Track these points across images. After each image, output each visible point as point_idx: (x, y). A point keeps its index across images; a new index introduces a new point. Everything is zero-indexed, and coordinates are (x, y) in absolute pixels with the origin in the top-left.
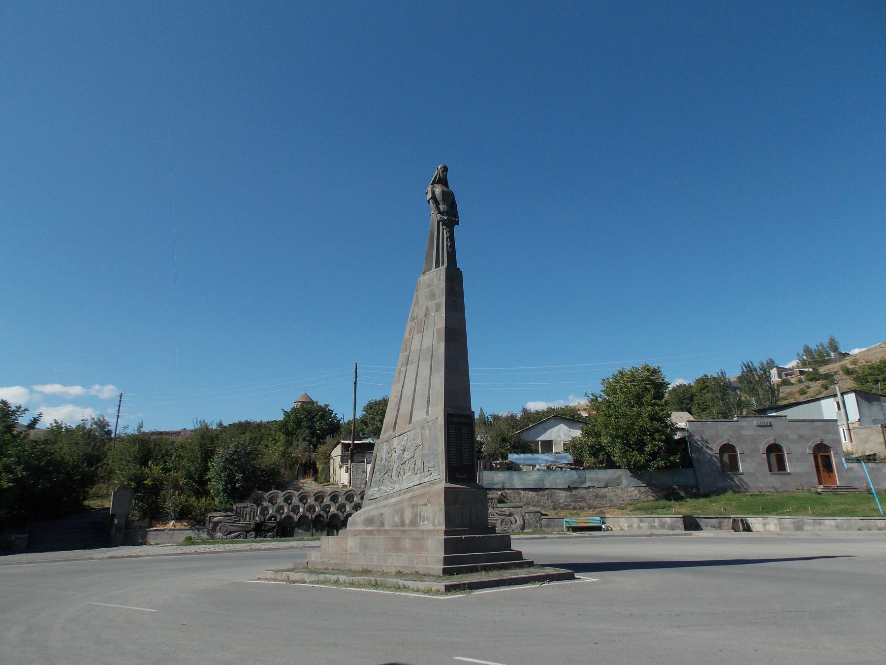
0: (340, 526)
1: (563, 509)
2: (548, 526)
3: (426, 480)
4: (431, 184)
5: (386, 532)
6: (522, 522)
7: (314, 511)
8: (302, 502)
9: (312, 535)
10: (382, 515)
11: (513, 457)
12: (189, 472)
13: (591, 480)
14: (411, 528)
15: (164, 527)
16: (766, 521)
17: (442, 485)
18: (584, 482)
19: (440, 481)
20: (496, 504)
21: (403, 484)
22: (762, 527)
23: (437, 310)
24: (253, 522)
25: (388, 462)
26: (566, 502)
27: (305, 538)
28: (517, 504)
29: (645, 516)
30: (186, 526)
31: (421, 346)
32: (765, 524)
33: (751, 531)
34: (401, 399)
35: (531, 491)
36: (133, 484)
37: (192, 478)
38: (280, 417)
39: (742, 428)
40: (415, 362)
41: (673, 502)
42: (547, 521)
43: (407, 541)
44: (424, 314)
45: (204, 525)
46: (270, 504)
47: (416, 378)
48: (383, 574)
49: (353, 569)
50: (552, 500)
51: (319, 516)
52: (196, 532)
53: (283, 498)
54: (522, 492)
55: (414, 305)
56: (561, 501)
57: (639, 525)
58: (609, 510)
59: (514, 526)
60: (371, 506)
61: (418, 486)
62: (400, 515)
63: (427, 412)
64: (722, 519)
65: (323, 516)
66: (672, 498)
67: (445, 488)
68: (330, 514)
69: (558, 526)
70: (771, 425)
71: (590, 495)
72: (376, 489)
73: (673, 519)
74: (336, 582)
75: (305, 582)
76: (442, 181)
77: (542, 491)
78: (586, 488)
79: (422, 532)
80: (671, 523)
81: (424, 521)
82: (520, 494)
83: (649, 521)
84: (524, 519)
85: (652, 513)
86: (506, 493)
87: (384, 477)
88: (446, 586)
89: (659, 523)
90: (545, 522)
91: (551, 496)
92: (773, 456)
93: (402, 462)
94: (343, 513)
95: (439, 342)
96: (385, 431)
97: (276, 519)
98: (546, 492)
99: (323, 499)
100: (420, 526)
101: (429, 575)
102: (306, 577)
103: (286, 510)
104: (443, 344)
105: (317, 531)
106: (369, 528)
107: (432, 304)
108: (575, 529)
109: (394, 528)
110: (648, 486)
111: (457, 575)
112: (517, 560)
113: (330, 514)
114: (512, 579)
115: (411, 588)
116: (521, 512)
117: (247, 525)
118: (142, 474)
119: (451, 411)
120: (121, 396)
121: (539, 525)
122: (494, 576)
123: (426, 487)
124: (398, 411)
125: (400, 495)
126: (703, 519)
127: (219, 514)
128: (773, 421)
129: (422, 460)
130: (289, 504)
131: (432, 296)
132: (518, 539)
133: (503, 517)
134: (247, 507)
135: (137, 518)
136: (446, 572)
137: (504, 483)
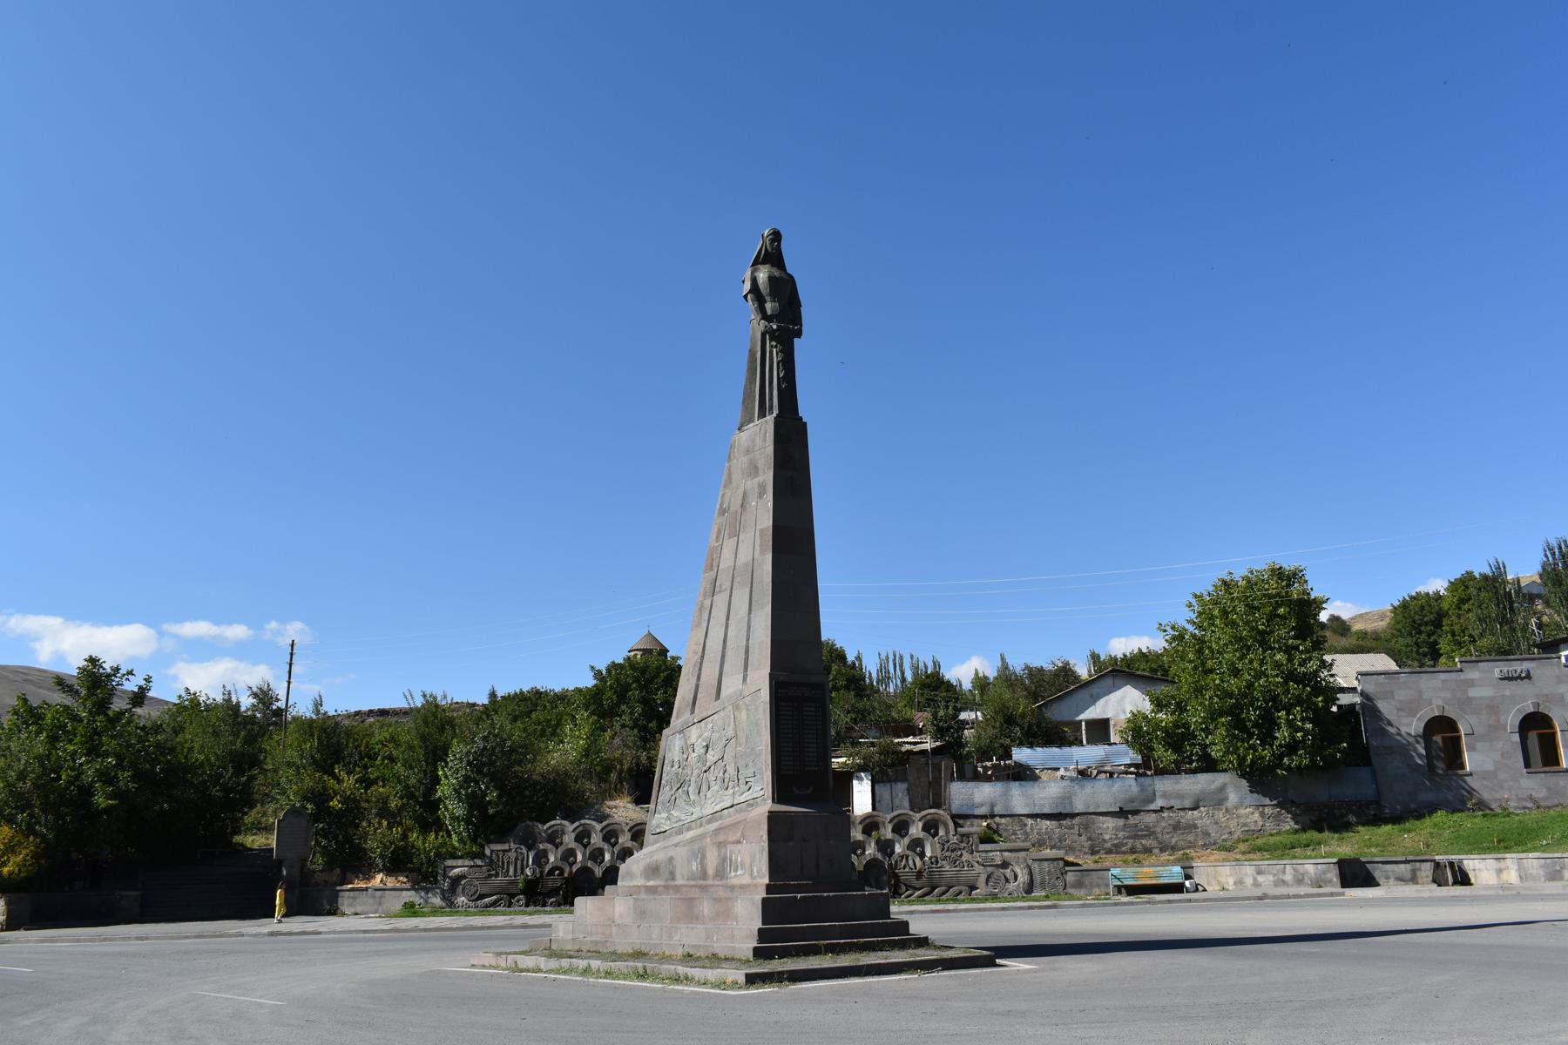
1: (1109, 852)
2: (1079, 884)
3: (742, 799)
4: (752, 266)
5: (677, 889)
6: (1027, 878)
10: (671, 859)
11: (1021, 755)
12: (407, 787)
13: (1165, 796)
14: (717, 883)
15: (366, 883)
16: (1502, 864)
17: (768, 806)
18: (1152, 800)
19: (764, 800)
20: (977, 846)
21: (706, 806)
22: (1495, 876)
23: (760, 497)
24: (521, 878)
25: (683, 769)
26: (1117, 838)
28: (1019, 844)
29: (1267, 862)
30: (405, 883)
31: (735, 561)
32: (1499, 871)
33: (1470, 884)
34: (703, 657)
35: (1050, 820)
36: (309, 806)
37: (411, 796)
38: (589, 682)
39: (1471, 683)
40: (725, 590)
41: (1326, 834)
42: (1076, 876)
43: (705, 904)
44: (740, 502)
45: (436, 881)
46: (549, 846)
47: (728, 619)
48: (665, 959)
49: (619, 952)
50: (1089, 835)
52: (423, 894)
53: (573, 836)
54: (1030, 821)
55: (725, 486)
56: (1107, 837)
57: (1255, 880)
58: (1201, 852)
59: (1012, 886)
60: (658, 845)
61: (731, 809)
62: (699, 860)
63: (745, 680)
64: (1418, 864)
66: (1326, 827)
67: (769, 812)
69: (1098, 886)
70: (1528, 677)
71: (1164, 824)
72: (665, 815)
73: (1319, 866)
74: (586, 971)
75: (540, 971)
76: (772, 255)
77: (1068, 819)
78: (1155, 811)
79: (733, 888)
80: (1315, 874)
81: (736, 870)
82: (1026, 825)
83: (1275, 872)
84: (1031, 874)
85: (1281, 857)
86: (998, 825)
87: (676, 795)
88: (747, 976)
89: (1294, 876)
90: (1074, 878)
91: (1086, 827)
92: (1533, 737)
93: (704, 769)
95: (762, 553)
96: (678, 713)
97: (562, 873)
98: (1077, 820)
100: (731, 878)
101: (733, 959)
102: (542, 962)
103: (579, 857)
104: (769, 557)
106: (651, 883)
107: (752, 484)
108: (1133, 890)
109: (692, 883)
110: (1279, 805)
111: (779, 958)
112: (900, 935)
114: (871, 965)
115: (697, 979)
116: (1025, 860)
118: (324, 788)
120: (292, 645)
121: (1060, 883)
122: (845, 960)
123: (741, 811)
124: (699, 678)
125: (701, 825)
126: (1380, 865)
127: (460, 862)
128: (1533, 669)
129: (736, 763)
130: (585, 847)
131: (753, 470)
132: (1003, 909)
133: (990, 869)
134: (510, 850)
135: (321, 868)
136: (759, 953)
137: (993, 806)
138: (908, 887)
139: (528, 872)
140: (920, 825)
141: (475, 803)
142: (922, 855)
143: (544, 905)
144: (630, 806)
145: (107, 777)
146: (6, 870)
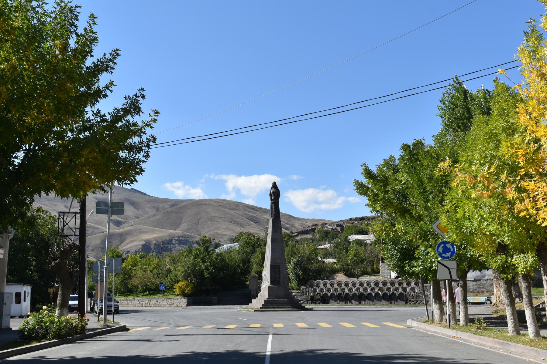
0: (351, 299)
7: (338, 291)
8: (332, 286)
9: (338, 303)
13: (488, 275)
18: (484, 277)
24: (310, 296)
26: (474, 288)
27: (335, 304)
36: (257, 275)
51: (340, 294)
53: (322, 284)
56: (471, 288)
65: (342, 294)
68: (345, 293)
71: (488, 284)
78: (485, 280)
94: (351, 292)
99: (341, 285)
105: (340, 301)
113: (345, 293)
117: (308, 297)
119: (272, 264)
127: (295, 291)
130: (326, 287)
136: (261, 308)
138: (410, 301)
139: (311, 294)
140: (414, 283)
141: (297, 275)
142: (414, 292)
143: (316, 303)
144: (343, 276)
145: (207, 268)
146: (186, 292)
